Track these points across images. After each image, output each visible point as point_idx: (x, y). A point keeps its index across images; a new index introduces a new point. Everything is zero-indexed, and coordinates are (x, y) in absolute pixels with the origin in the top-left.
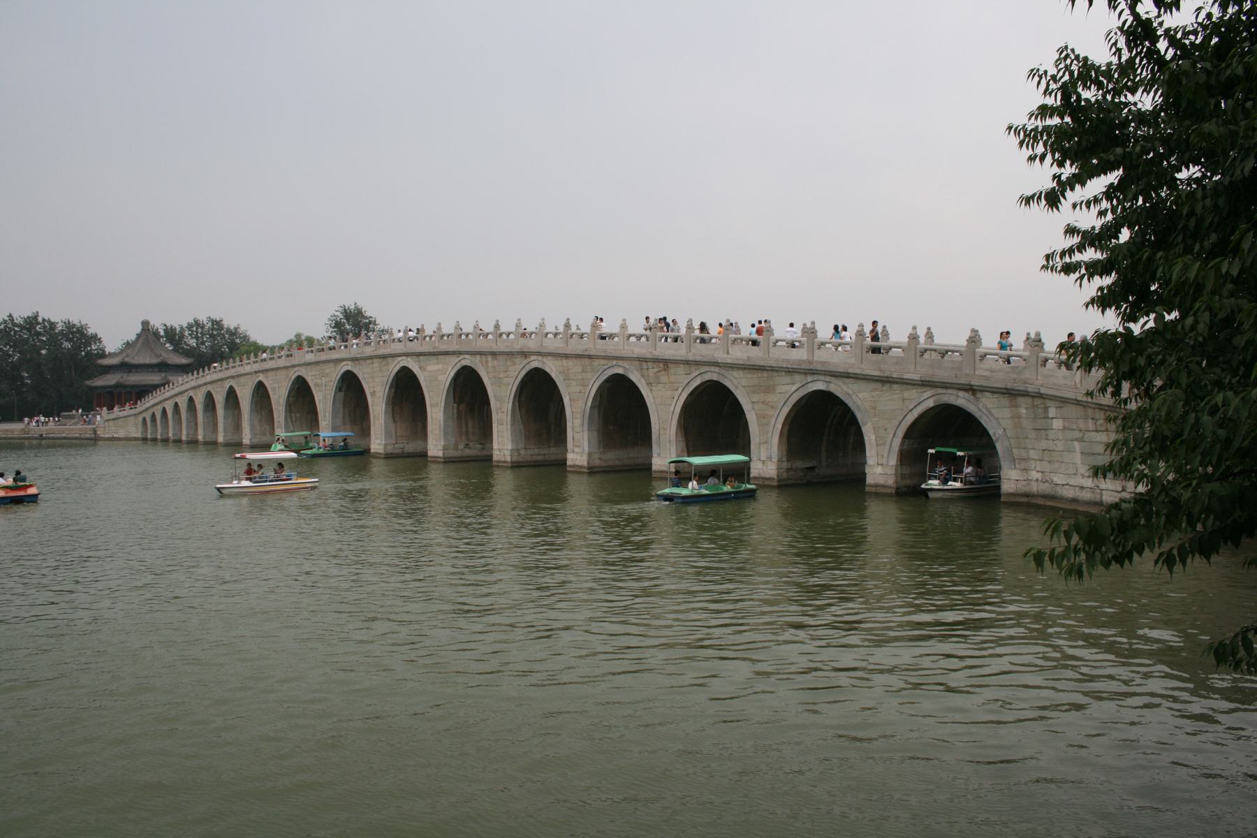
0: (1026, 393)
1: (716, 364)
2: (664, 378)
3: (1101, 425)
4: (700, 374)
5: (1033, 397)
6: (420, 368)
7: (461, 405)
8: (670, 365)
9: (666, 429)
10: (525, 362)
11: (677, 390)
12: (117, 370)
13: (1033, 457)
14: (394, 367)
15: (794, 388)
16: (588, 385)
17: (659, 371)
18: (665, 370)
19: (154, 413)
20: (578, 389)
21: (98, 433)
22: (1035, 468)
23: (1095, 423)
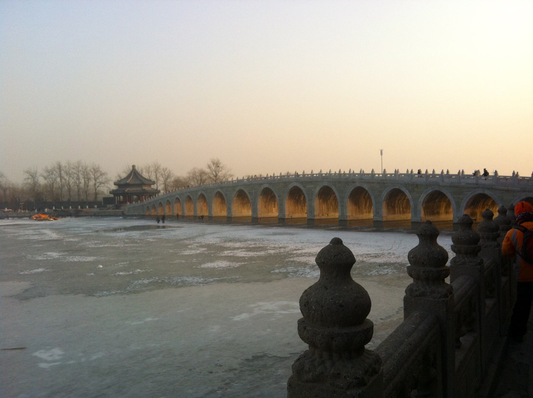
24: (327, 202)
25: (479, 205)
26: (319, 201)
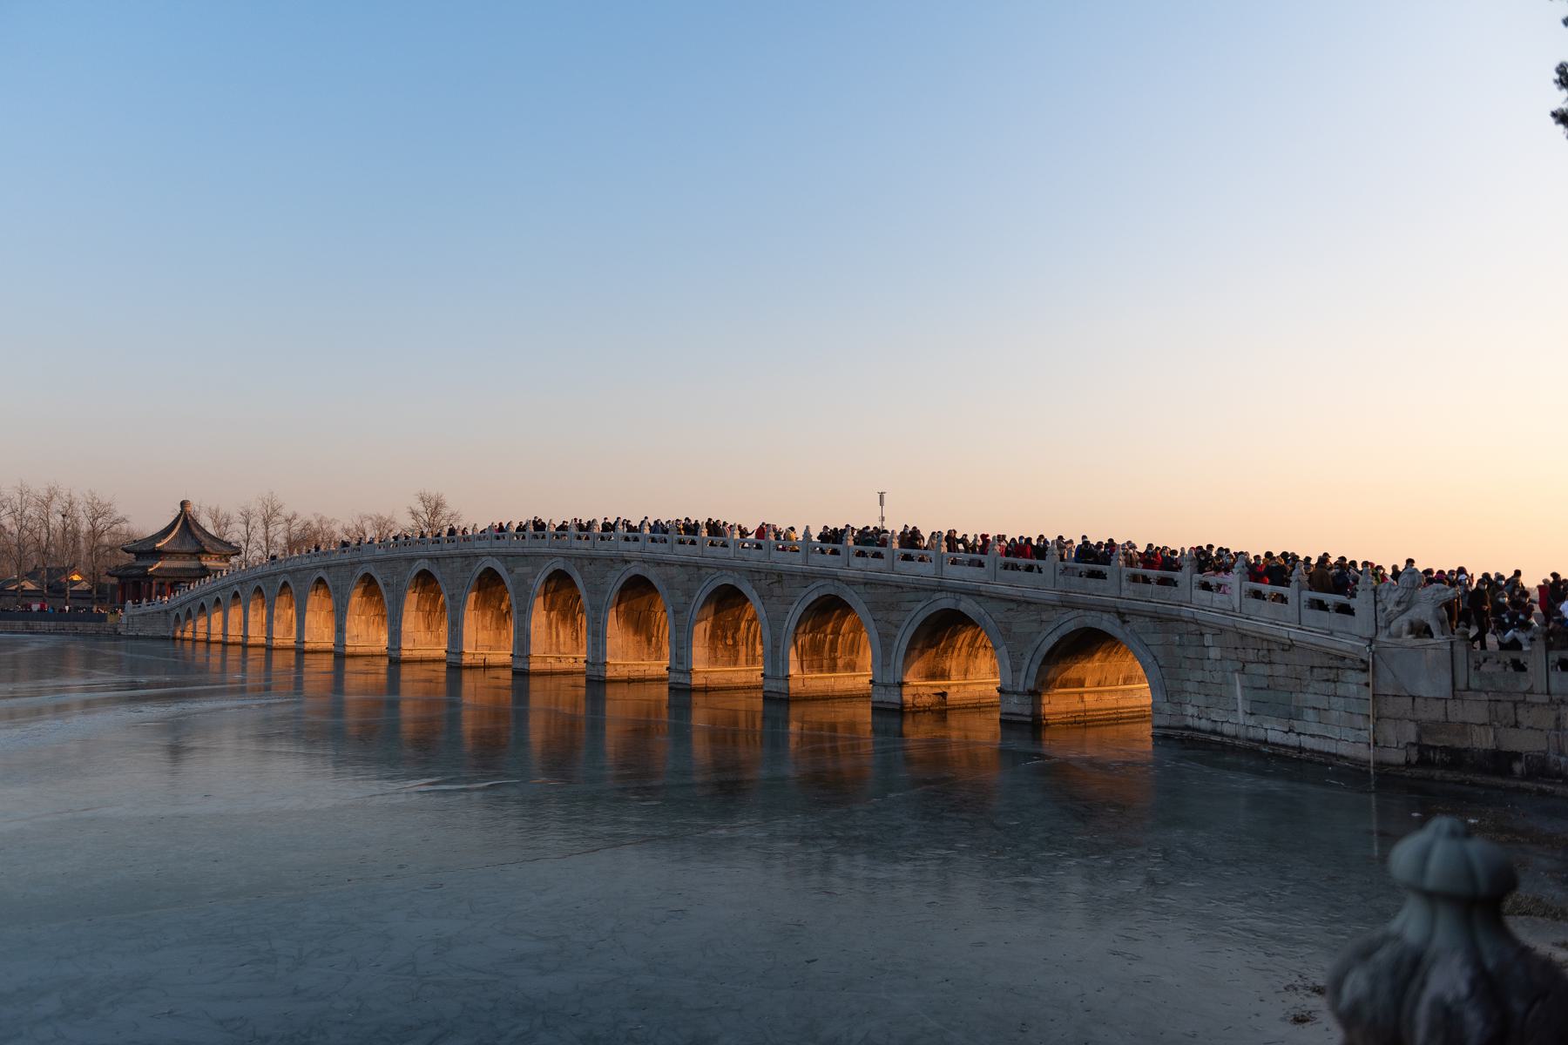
0: (1179, 618)
1: (835, 577)
2: (777, 591)
3: (1263, 656)
4: (817, 587)
5: (1187, 622)
6: (507, 570)
7: (552, 613)
8: (784, 577)
9: (778, 647)
10: (625, 568)
11: (792, 604)
12: (148, 558)
13: (1190, 689)
14: (478, 569)
15: (920, 606)
16: (694, 596)
17: (772, 583)
18: (779, 582)
19: (189, 608)
20: (683, 599)
21: (119, 630)
22: (1190, 701)
23: (1258, 654)
24: (574, 619)
25: (958, 645)
26: (548, 616)
